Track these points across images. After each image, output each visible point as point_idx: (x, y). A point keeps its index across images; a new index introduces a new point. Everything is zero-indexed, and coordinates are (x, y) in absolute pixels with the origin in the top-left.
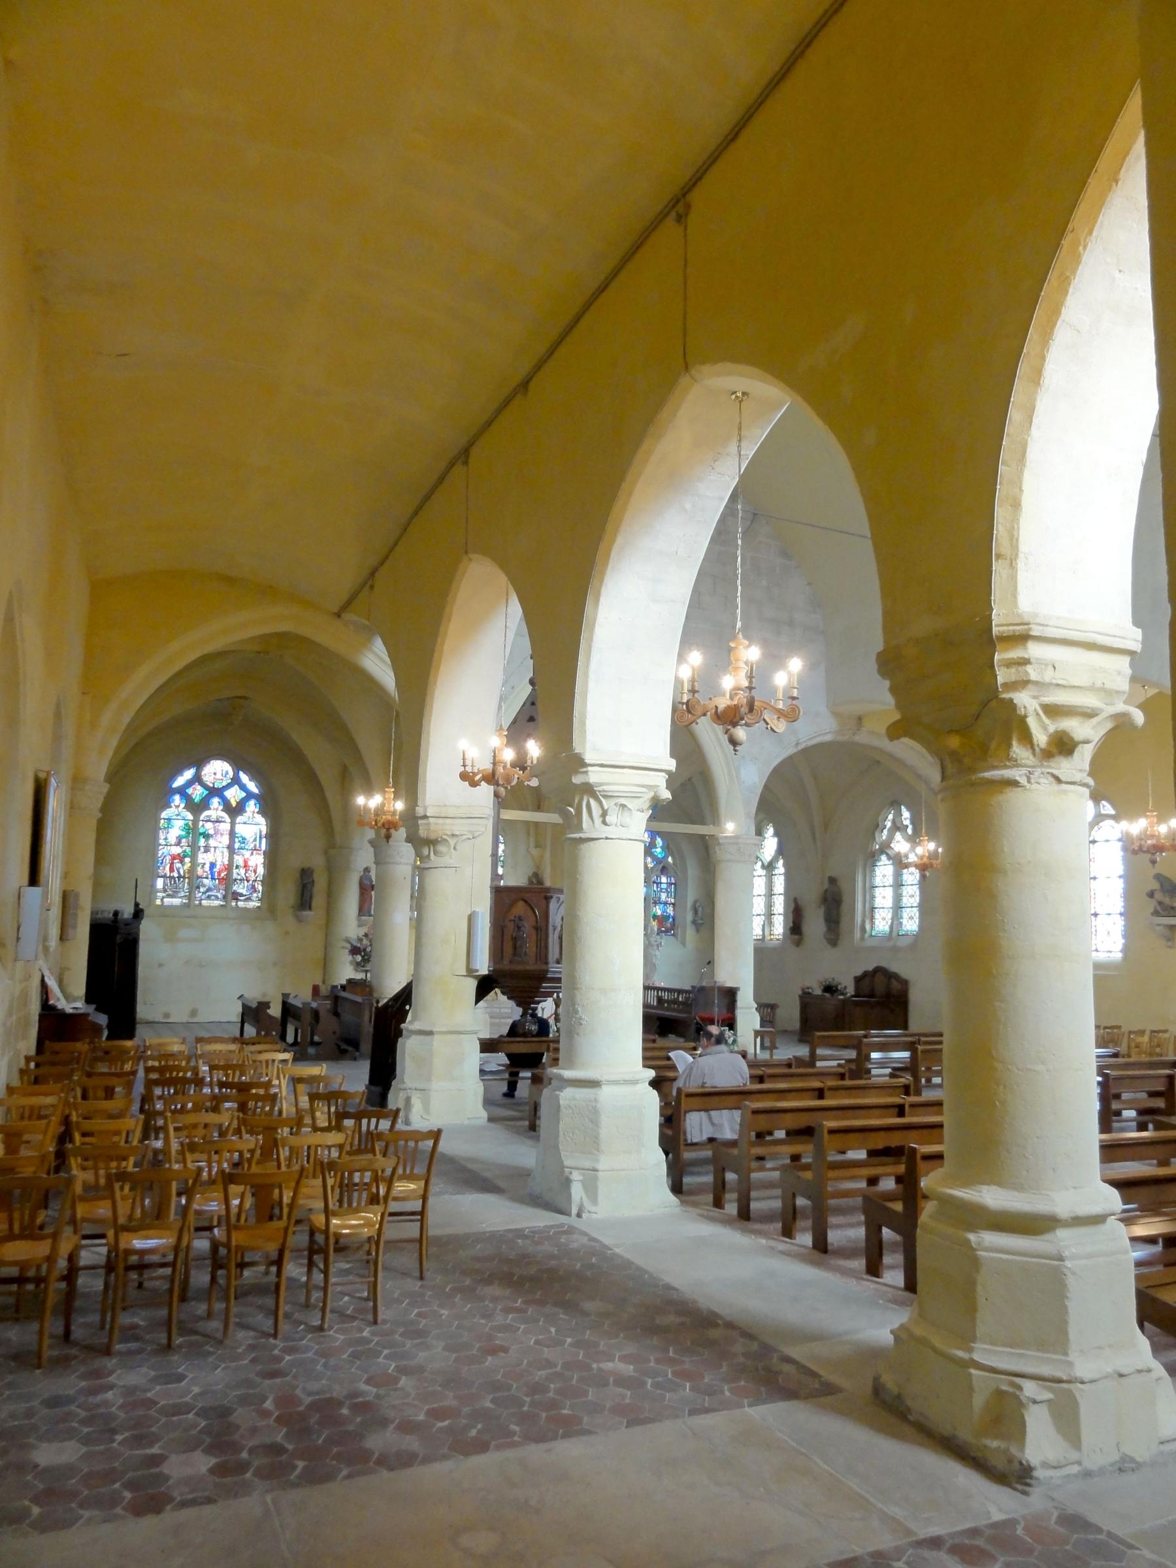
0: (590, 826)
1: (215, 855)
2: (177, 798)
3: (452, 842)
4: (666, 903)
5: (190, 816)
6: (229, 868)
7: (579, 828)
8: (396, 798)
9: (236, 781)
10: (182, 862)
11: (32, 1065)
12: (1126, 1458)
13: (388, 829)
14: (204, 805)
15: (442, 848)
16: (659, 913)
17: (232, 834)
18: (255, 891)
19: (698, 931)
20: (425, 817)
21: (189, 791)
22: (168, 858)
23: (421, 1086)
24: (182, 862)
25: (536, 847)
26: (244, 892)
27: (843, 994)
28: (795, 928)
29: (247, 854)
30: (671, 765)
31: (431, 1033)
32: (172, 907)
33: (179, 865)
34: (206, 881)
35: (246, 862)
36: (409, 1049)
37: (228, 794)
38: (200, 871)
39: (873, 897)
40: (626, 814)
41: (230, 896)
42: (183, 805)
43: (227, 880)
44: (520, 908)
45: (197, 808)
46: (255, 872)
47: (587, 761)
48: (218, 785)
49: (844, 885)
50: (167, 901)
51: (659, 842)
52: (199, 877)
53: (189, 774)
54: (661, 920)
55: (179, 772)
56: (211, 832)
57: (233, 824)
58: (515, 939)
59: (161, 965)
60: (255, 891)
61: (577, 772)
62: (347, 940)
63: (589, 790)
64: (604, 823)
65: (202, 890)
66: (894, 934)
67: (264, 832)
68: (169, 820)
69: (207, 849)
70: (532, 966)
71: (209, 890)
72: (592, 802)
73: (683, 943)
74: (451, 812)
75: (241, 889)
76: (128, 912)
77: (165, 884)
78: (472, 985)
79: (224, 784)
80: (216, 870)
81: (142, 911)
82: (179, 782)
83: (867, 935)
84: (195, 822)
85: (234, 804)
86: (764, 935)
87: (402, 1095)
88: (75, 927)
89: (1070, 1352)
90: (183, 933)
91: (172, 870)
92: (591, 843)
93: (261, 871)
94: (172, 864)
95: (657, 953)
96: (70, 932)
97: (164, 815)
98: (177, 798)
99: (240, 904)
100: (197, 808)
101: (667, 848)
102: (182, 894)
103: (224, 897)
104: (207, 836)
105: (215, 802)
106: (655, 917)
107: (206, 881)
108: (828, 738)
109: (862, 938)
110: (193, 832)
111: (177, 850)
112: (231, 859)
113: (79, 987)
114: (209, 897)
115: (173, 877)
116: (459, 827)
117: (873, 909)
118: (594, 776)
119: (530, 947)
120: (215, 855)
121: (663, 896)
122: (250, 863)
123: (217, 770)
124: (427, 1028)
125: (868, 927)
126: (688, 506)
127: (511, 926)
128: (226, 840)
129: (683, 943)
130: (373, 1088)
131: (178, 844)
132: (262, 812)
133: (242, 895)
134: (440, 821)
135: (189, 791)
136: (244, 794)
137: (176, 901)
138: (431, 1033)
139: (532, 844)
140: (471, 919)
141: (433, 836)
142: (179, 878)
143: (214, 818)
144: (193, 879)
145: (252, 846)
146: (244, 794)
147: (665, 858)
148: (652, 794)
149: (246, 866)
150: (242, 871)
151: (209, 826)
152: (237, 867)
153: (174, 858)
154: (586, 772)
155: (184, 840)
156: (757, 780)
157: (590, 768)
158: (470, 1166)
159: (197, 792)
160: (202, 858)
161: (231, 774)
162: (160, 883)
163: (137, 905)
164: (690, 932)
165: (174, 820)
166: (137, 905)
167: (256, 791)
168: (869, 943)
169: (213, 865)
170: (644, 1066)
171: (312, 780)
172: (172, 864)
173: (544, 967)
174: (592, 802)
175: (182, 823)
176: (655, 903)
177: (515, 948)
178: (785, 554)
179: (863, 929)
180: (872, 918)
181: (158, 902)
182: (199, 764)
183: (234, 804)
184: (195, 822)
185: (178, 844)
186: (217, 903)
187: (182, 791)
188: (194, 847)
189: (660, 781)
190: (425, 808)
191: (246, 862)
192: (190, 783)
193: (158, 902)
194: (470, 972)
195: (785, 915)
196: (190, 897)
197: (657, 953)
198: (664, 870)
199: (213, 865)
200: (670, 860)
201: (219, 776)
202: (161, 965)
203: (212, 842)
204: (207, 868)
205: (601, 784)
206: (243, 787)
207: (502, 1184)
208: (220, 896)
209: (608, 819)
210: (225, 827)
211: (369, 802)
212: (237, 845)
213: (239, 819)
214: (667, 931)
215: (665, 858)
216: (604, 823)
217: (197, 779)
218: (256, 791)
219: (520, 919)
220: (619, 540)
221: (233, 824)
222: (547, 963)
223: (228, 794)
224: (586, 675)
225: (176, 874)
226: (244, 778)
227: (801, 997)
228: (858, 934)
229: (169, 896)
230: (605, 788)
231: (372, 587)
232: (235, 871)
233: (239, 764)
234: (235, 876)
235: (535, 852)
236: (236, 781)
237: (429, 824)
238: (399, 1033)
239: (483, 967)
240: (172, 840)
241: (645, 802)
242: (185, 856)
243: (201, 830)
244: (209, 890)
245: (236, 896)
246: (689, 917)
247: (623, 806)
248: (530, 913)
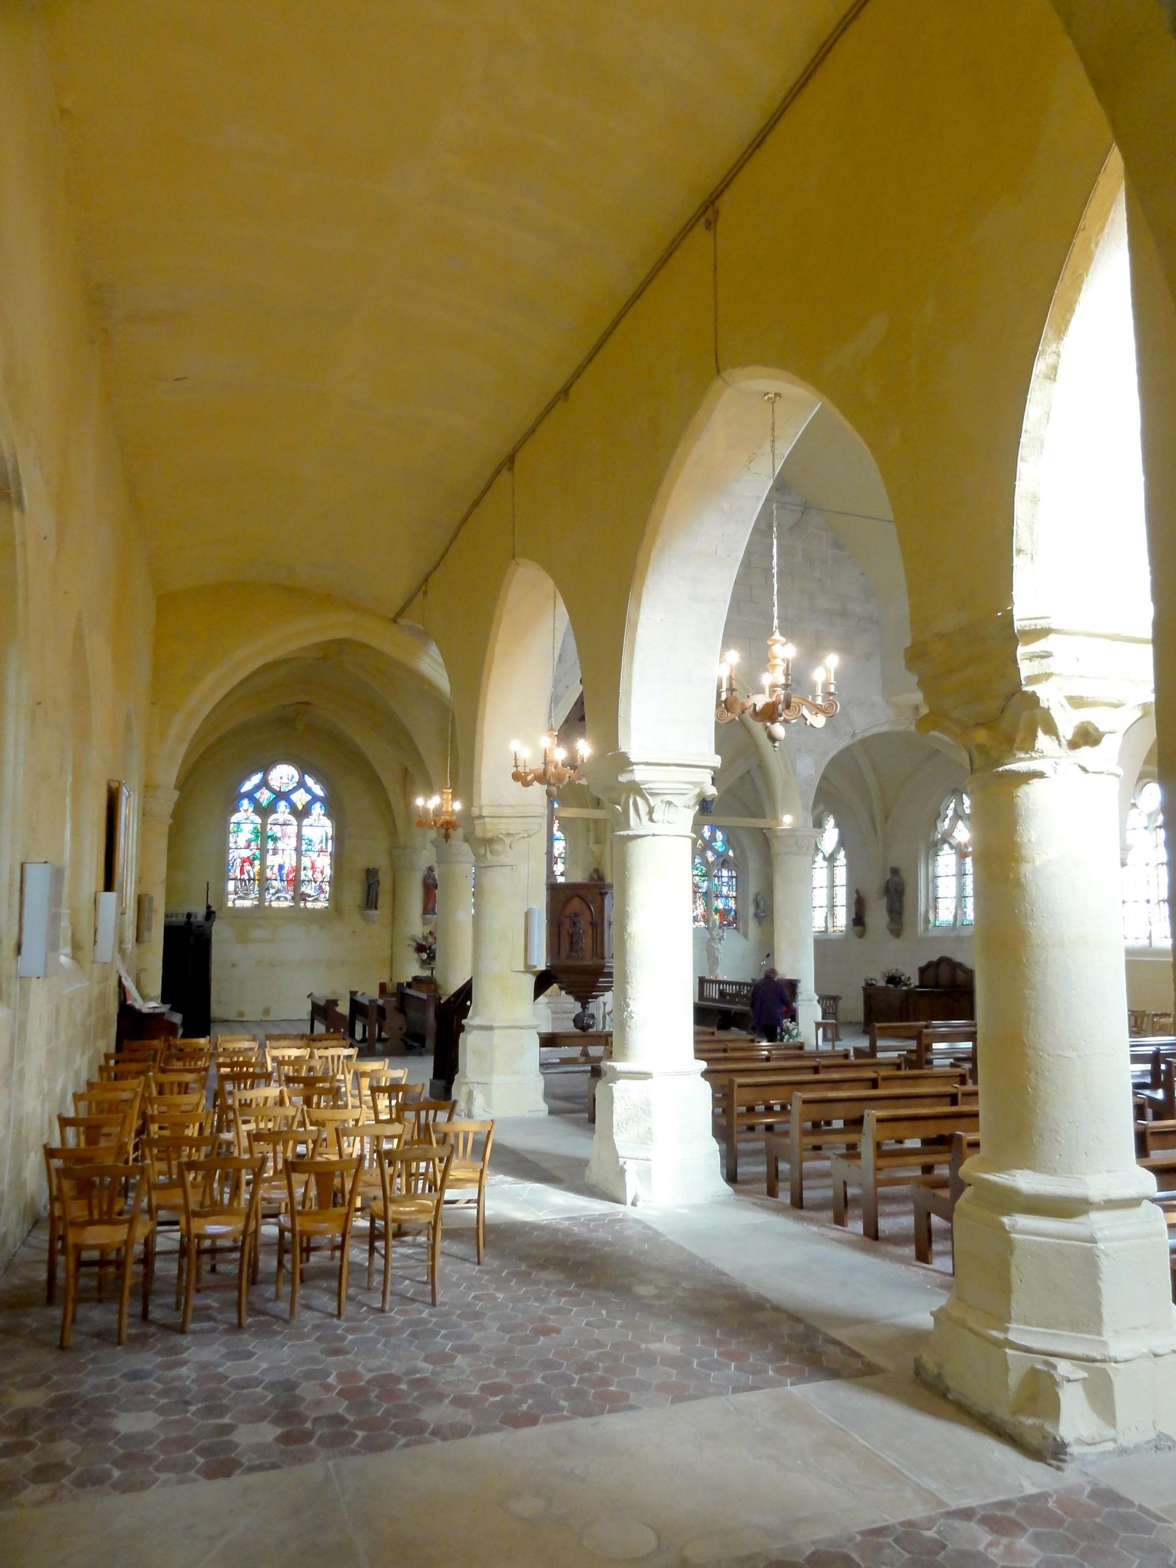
0: (637, 824)
1: (283, 857)
2: (245, 803)
3: (507, 841)
4: (727, 897)
5: (258, 820)
6: (297, 869)
7: (627, 826)
8: (454, 798)
9: (301, 784)
10: (251, 864)
11: (112, 1062)
12: (1161, 1436)
13: (447, 830)
14: (271, 808)
15: (498, 847)
16: (721, 906)
17: (299, 836)
18: (323, 891)
20: (481, 817)
21: (257, 795)
22: (239, 861)
23: (483, 1080)
24: (251, 864)
25: (597, 842)
26: (312, 893)
27: (906, 985)
28: (858, 919)
29: (314, 855)
30: (717, 761)
31: (490, 1028)
32: (244, 910)
33: (249, 868)
34: (275, 883)
35: (313, 864)
36: (470, 1044)
37: (295, 797)
38: (269, 874)
39: (936, 887)
40: (673, 810)
41: (298, 897)
42: (251, 809)
43: (296, 882)
44: (576, 905)
45: (264, 812)
46: (322, 873)
47: (633, 760)
48: (284, 789)
49: (905, 875)
50: (239, 903)
51: (719, 835)
52: (268, 879)
53: (256, 779)
54: (723, 913)
55: (247, 777)
56: (279, 835)
57: (300, 827)
58: (571, 936)
59: (234, 965)
60: (323, 891)
61: (623, 771)
62: (413, 939)
63: (635, 788)
64: (651, 820)
65: (272, 891)
66: (958, 924)
67: (330, 835)
68: (238, 823)
69: (275, 852)
70: (588, 962)
71: (278, 891)
72: (639, 799)
73: (746, 936)
74: (507, 811)
75: (308, 889)
76: (201, 912)
77: (236, 887)
78: (530, 982)
79: (291, 787)
80: (285, 872)
81: (214, 912)
82: (247, 786)
83: (931, 926)
84: (264, 825)
85: (300, 807)
86: (826, 927)
87: (464, 1089)
88: (149, 929)
89: (1104, 1333)
90: (256, 934)
91: (242, 872)
92: (639, 840)
93: (328, 872)
94: (242, 867)
95: (719, 946)
96: (146, 935)
97: (234, 819)
98: (245, 803)
99: (309, 905)
100: (264, 812)
101: (727, 842)
102: (253, 896)
103: (293, 898)
104: (275, 839)
105: (282, 805)
106: (717, 911)
107: (275, 883)
108: (885, 728)
109: (926, 929)
110: (262, 835)
111: (246, 853)
112: (299, 861)
113: (155, 985)
114: (278, 898)
115: (242, 880)
116: (514, 826)
117: (936, 899)
118: (640, 774)
119: (587, 942)
120: (283, 857)
121: (725, 890)
122: (317, 865)
123: (283, 775)
124: (488, 1024)
125: (931, 917)
126: (726, 506)
127: (567, 924)
128: (293, 843)
130: (437, 1082)
131: (248, 847)
132: (328, 814)
133: (310, 896)
134: (495, 820)
135: (257, 795)
136: (309, 797)
137: (247, 903)
138: (490, 1028)
139: (592, 839)
140: (528, 916)
141: (489, 835)
142: (249, 880)
143: (281, 821)
144: (263, 881)
145: (318, 847)
146: (309, 797)
147: (726, 851)
148: (698, 790)
149: (313, 867)
150: (309, 873)
151: (277, 830)
152: (305, 869)
153: (244, 861)
154: (632, 771)
155: (253, 844)
156: (813, 772)
157: (635, 767)
158: (529, 1157)
159: (265, 797)
160: (271, 860)
161: (297, 778)
162: (231, 886)
163: (209, 907)
164: (752, 925)
165: (244, 820)
166: (209, 907)
167: (321, 793)
168: (932, 933)
169: (281, 867)
170: (696, 1058)
171: (374, 782)
172: (242, 867)
173: (599, 962)
174: (639, 799)
175: (251, 826)
176: (717, 897)
177: (571, 943)
178: (837, 545)
179: (927, 921)
180: (936, 908)
181: (230, 904)
182: (266, 769)
183: (300, 807)
184: (264, 825)
185: (248, 847)
186: (285, 904)
187: (250, 795)
188: (263, 851)
189: (706, 777)
190: (481, 808)
191: (313, 864)
192: (257, 788)
193: (230, 904)
194: (528, 968)
195: (848, 906)
196: (261, 898)
197: (719, 946)
198: (724, 863)
199: (281, 867)
200: (731, 853)
201: (285, 780)
202: (234, 965)
203: (280, 845)
204: (276, 870)
205: (646, 782)
206: (308, 791)
207: (558, 1173)
208: (289, 897)
209: (654, 816)
210: (292, 830)
211: (428, 803)
212: (304, 847)
213: (306, 822)
214: (729, 924)
215: (726, 851)
216: (651, 820)
217: (264, 783)
218: (321, 793)
219: (576, 915)
220: (659, 543)
221: (300, 827)
222: (603, 958)
223: (295, 797)
224: (630, 676)
225: (246, 877)
226: (309, 781)
227: (864, 989)
228: (921, 926)
229: (240, 898)
230: (651, 785)
231: (425, 593)
232: (303, 873)
233: (304, 769)
234: (303, 877)
235: (595, 848)
236: (301, 784)
237: (484, 824)
238: (461, 1028)
239: (541, 964)
240: (242, 843)
241: (691, 798)
242: (254, 859)
243: (270, 833)
244: (278, 891)
245: (304, 897)
246: (751, 910)
247: (669, 803)
248: (585, 908)
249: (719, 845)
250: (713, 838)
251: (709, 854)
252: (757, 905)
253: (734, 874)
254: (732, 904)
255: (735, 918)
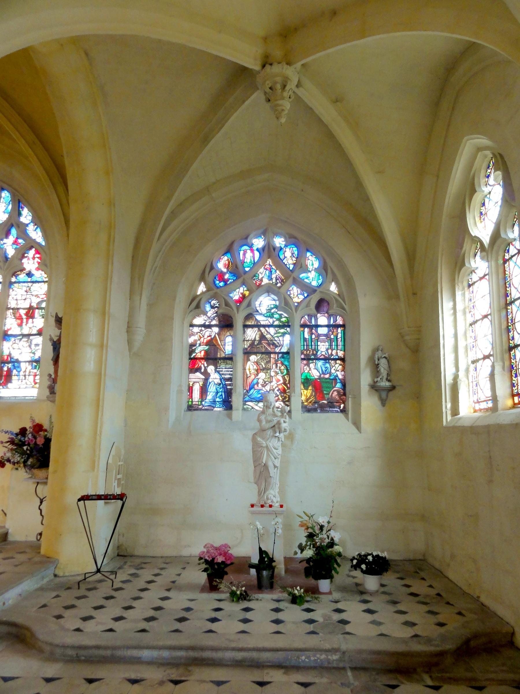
4: (327, 359)
16: (315, 374)
19: (383, 402)
51: (312, 262)
73: (357, 424)
86: (494, 398)
101: (324, 270)
106: (307, 382)
121: (323, 348)
129: (357, 424)
164: (369, 405)
176: (308, 359)
198: (321, 305)
200: (333, 288)
214: (331, 404)
246: (366, 378)
249: (312, 278)
250: (300, 265)
251: (295, 291)
252: (375, 368)
253: (340, 321)
254: (337, 370)
255: (343, 393)
